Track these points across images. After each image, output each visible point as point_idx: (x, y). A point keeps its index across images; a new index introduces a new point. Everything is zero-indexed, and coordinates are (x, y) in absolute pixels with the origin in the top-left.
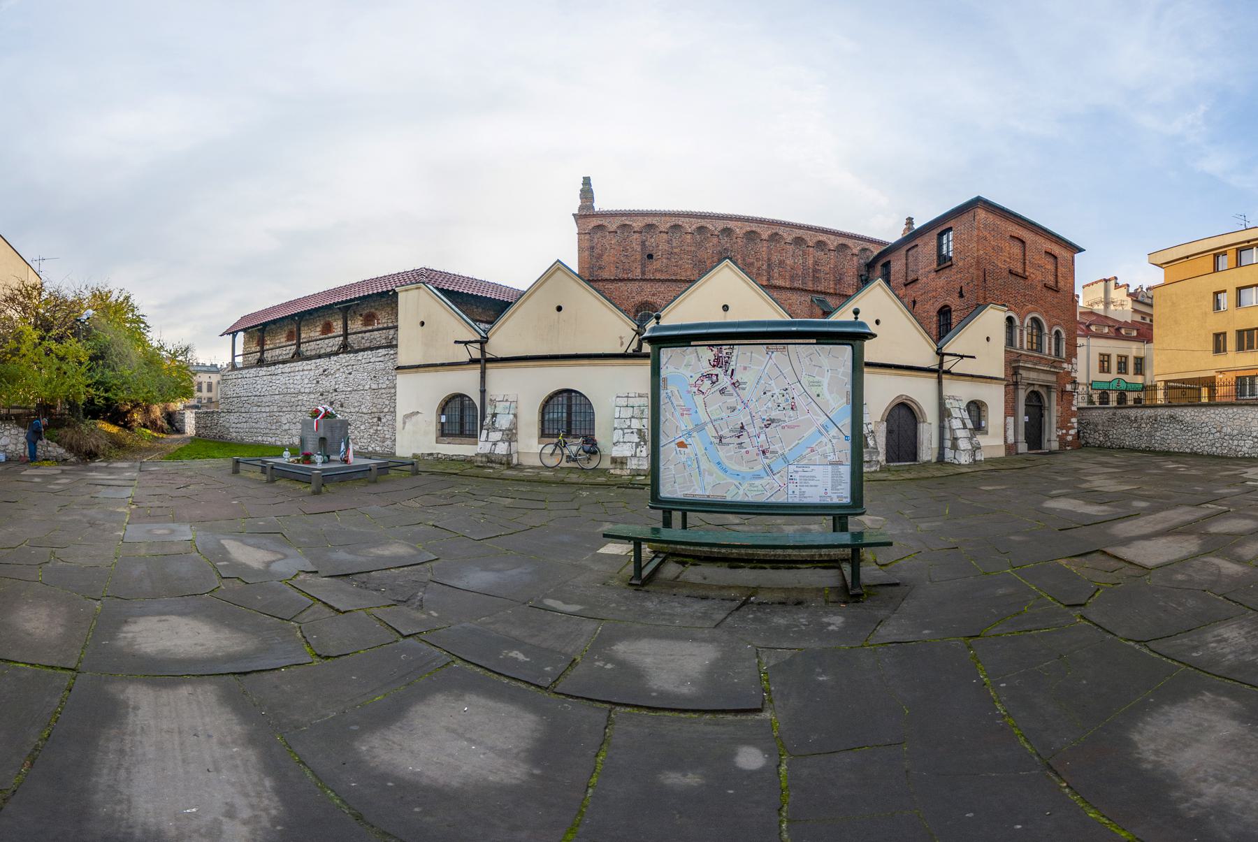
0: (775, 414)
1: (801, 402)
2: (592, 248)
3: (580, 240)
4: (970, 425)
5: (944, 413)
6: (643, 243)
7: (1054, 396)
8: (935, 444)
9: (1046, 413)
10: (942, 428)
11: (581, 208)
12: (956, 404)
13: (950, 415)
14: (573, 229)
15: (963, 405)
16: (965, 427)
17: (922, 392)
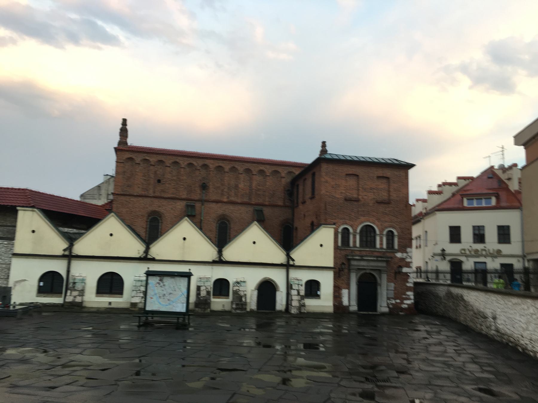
0: (172, 292)
1: (177, 289)
2: (124, 172)
3: (117, 167)
4: (302, 293)
5: (289, 287)
6: (155, 172)
7: (384, 277)
8: (284, 302)
9: (379, 288)
10: (288, 294)
11: (120, 143)
12: (297, 282)
13: (292, 288)
14: (113, 157)
15: (303, 283)
16: (299, 294)
17: (278, 277)
